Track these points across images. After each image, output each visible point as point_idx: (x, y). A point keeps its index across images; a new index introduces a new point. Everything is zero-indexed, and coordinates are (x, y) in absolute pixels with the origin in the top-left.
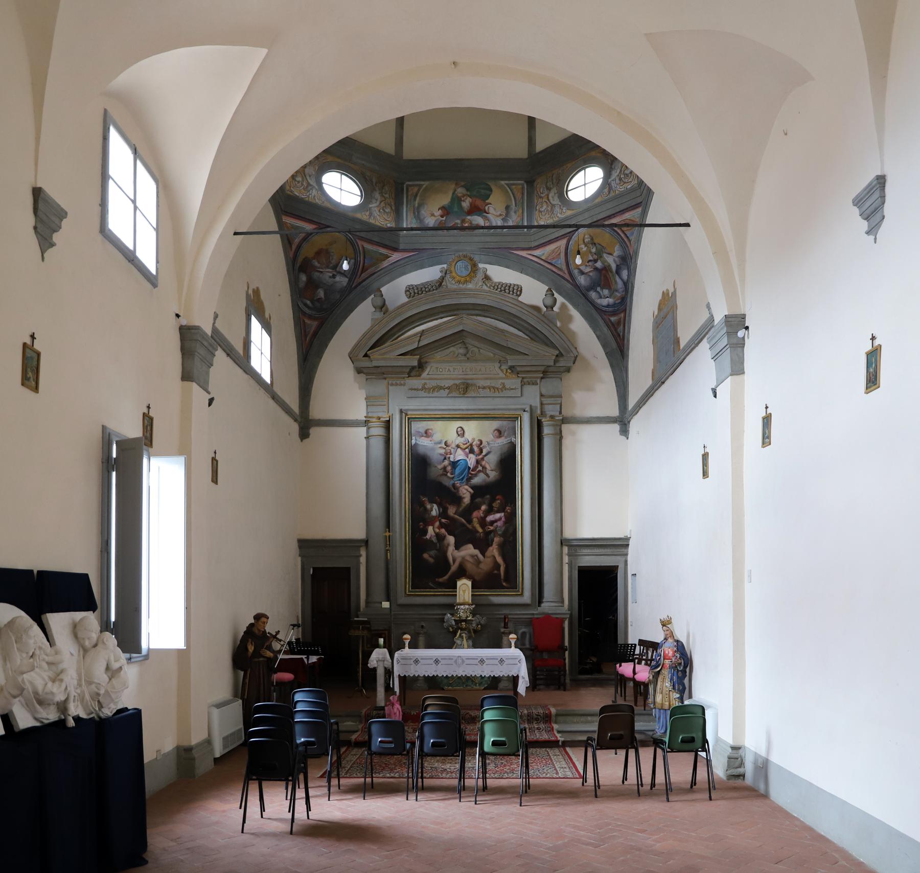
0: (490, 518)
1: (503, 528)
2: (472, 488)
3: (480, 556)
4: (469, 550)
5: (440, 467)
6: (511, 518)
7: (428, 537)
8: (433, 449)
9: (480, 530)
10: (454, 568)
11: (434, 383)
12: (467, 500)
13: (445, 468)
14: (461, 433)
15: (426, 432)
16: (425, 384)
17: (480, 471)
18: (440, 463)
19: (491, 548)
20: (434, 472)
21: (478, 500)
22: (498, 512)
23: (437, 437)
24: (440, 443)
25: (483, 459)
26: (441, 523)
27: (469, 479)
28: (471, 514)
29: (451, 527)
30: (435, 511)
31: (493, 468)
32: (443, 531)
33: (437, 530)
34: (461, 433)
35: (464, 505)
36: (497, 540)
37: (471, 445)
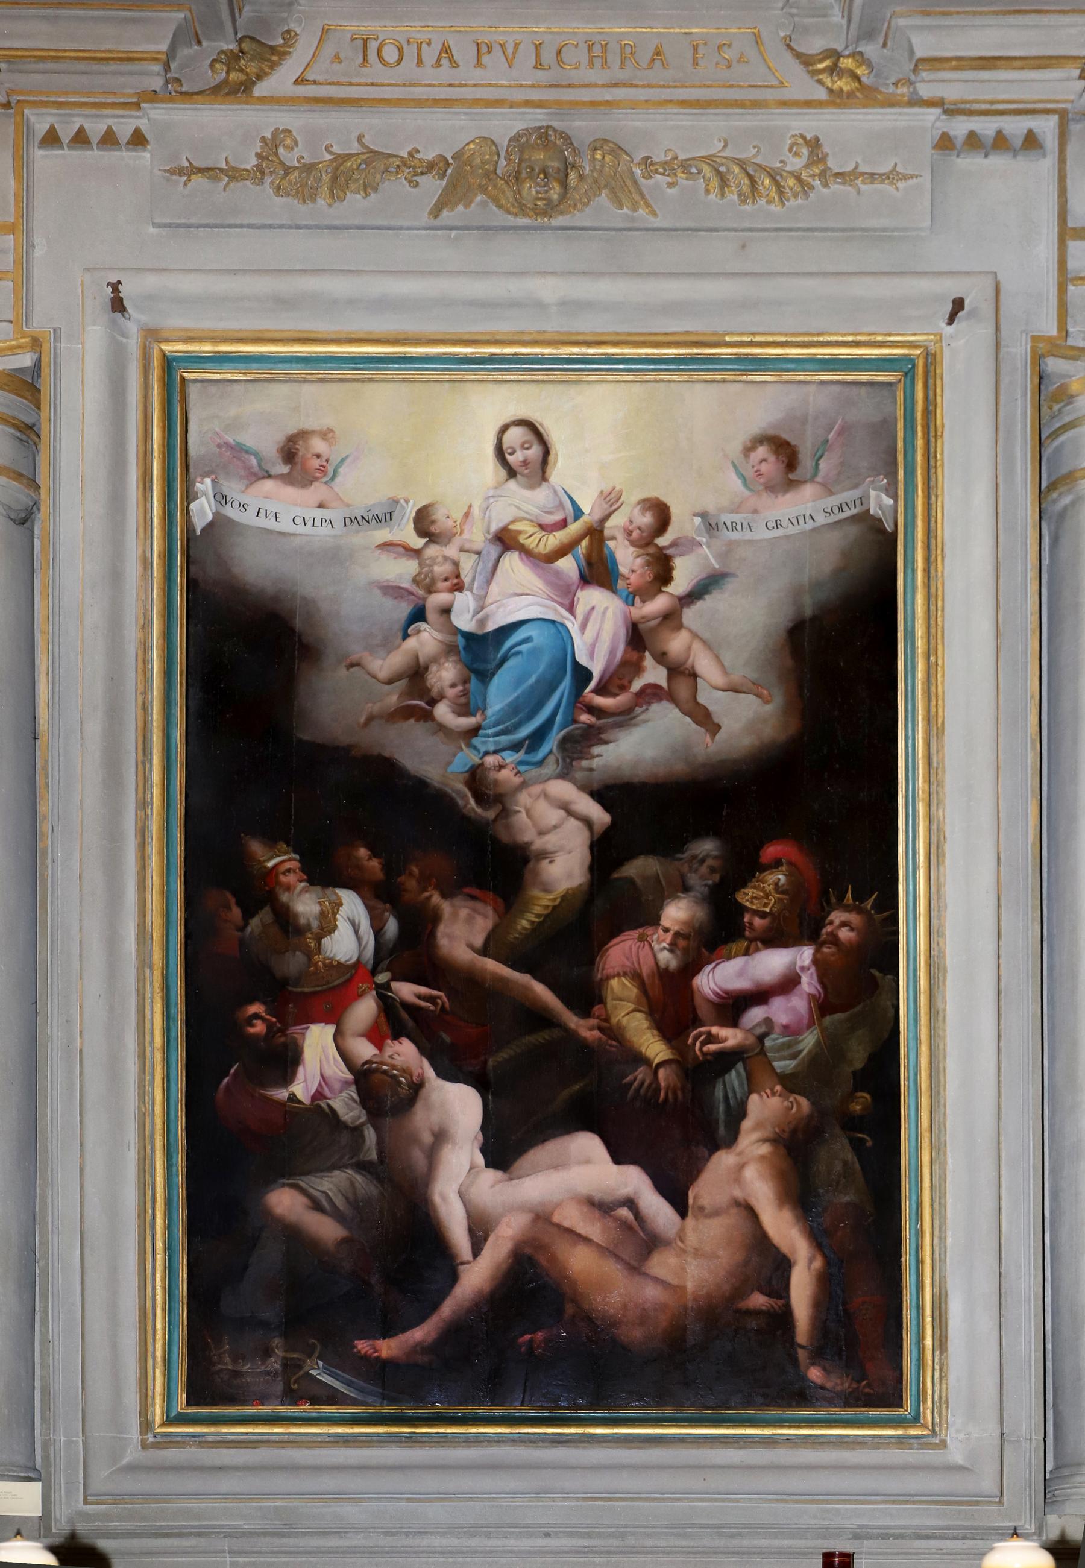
0: (720, 977)
1: (809, 1041)
2: (602, 794)
3: (657, 1208)
4: (579, 1170)
6: (864, 983)
7: (302, 1088)
8: (334, 557)
9: (656, 1049)
10: (476, 1275)
11: (342, 132)
12: (565, 867)
13: (416, 675)
14: (526, 454)
15: (290, 453)
16: (273, 143)
17: (652, 693)
18: (387, 646)
19: (723, 1160)
20: (344, 702)
21: (640, 868)
22: (774, 939)
23: (362, 483)
24: (385, 517)
25: (671, 618)
26: (388, 1005)
27: (578, 744)
29: (465, 1031)
30: (348, 930)
31: (741, 672)
32: (404, 1053)
33: (364, 1050)
34: (526, 454)
35: (541, 902)
36: (765, 1109)
37: (596, 533)
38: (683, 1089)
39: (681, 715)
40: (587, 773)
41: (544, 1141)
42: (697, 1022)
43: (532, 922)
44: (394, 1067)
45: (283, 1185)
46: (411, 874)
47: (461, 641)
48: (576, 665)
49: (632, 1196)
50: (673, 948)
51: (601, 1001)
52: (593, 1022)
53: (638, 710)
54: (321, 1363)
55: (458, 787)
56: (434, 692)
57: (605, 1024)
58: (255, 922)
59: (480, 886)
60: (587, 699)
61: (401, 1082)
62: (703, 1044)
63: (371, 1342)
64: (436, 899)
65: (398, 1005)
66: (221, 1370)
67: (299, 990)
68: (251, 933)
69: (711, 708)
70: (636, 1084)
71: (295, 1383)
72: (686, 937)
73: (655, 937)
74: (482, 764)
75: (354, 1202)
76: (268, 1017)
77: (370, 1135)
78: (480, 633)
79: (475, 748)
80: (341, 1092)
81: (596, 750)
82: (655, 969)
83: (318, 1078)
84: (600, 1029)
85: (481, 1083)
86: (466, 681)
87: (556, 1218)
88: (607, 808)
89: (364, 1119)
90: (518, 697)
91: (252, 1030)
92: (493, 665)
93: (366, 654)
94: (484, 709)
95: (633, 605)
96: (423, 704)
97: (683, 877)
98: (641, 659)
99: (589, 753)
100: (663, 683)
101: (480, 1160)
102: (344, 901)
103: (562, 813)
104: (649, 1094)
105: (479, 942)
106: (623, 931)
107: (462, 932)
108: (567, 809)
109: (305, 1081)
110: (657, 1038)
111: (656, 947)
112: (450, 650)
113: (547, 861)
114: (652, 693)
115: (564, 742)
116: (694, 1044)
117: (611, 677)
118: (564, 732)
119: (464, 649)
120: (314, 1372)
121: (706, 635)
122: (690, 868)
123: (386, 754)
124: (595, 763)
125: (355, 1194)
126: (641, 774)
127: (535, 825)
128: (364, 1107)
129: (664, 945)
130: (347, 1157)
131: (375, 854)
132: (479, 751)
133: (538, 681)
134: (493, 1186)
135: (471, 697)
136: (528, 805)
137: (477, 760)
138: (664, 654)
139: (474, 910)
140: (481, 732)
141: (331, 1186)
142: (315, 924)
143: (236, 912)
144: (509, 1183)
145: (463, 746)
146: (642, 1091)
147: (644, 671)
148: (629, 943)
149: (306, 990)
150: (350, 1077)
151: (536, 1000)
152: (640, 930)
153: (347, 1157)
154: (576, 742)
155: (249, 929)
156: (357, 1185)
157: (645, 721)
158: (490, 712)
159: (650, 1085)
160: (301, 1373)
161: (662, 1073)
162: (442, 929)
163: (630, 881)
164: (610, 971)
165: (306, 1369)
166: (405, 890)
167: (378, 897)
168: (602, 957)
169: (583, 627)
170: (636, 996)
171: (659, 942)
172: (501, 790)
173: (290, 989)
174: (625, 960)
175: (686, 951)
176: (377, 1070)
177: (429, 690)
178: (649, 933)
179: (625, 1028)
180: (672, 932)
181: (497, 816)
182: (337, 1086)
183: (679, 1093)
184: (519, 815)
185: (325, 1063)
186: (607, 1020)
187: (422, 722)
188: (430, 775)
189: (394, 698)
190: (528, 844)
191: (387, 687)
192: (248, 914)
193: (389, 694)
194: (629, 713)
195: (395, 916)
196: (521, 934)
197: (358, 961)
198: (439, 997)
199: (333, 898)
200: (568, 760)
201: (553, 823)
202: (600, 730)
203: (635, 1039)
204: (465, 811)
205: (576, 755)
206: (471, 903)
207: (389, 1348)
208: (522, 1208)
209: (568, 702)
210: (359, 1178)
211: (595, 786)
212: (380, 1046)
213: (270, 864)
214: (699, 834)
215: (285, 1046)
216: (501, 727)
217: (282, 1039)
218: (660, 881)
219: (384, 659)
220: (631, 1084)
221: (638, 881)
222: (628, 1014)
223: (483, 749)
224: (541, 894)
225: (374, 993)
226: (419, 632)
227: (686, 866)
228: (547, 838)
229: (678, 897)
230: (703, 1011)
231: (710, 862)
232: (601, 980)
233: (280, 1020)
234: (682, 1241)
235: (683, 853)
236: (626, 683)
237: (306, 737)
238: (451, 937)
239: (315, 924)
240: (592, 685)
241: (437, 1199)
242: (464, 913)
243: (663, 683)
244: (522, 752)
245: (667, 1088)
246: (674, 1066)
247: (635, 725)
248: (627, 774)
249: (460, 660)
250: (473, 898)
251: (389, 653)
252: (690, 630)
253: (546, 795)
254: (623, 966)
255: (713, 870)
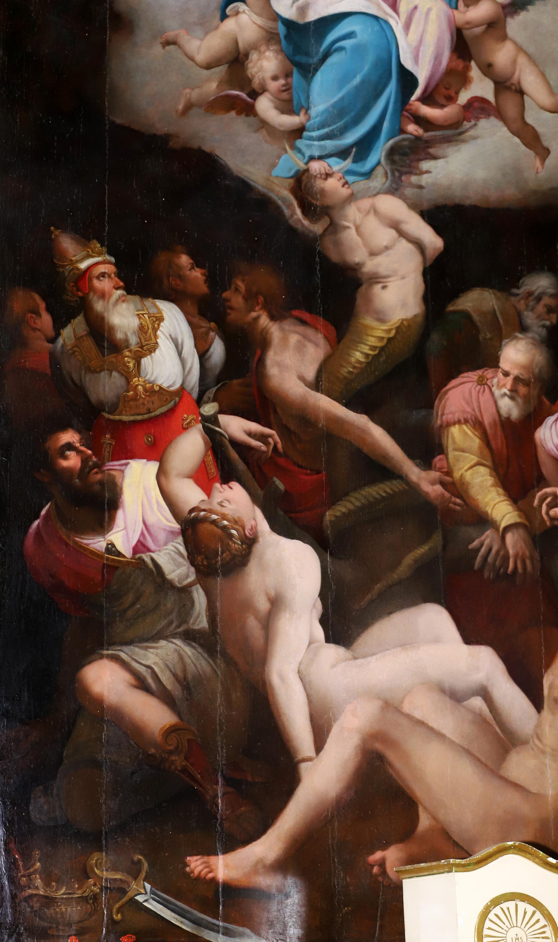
5: (205, 45)
7: (122, 536)
9: (501, 510)
10: (323, 777)
13: (235, 61)
17: (478, 108)
18: (205, 26)
21: (476, 301)
26: (216, 441)
27: (407, 157)
28: (427, 396)
29: (301, 478)
30: (170, 351)
32: (235, 501)
33: (191, 495)
38: (532, 558)
39: (510, 134)
40: (416, 190)
41: (390, 613)
42: (542, 481)
43: (367, 355)
44: (224, 517)
45: (102, 657)
46: (237, 290)
47: (282, 30)
48: (402, 69)
49: (485, 682)
50: (513, 394)
51: (441, 450)
52: (434, 475)
53: (467, 125)
54: (148, 886)
55: (283, 194)
56: (256, 83)
57: (448, 479)
58: (67, 332)
59: (310, 311)
60: (413, 108)
61: (231, 536)
62: (551, 506)
63: (206, 859)
64: (264, 320)
65: (227, 443)
66: (31, 896)
67: (117, 417)
68: (63, 346)
69: (540, 130)
70: (483, 550)
71: (118, 911)
72: (527, 383)
73: (495, 381)
74: (307, 170)
75: (184, 682)
76: (83, 448)
77: (199, 597)
78: (301, 22)
79: (300, 151)
80: (166, 544)
81: (425, 165)
82: (497, 418)
83: (141, 525)
84: (443, 484)
85: (320, 542)
86: (288, 75)
87: (407, 708)
88: (438, 230)
89: (192, 577)
90: (342, 98)
91: (65, 463)
92: (315, 60)
93: (182, 32)
94: (307, 109)
95: (456, 8)
96: (244, 95)
97: (519, 314)
98: (467, 68)
99: (418, 168)
100: (491, 97)
101: (320, 633)
102: (165, 316)
103: (393, 233)
104: (498, 563)
105: (311, 374)
106: (463, 373)
107: (293, 361)
108: (396, 226)
109: (125, 528)
110: (503, 498)
111: (497, 393)
112: (271, 37)
113: (380, 286)
114: (478, 108)
115: (392, 153)
116: (540, 506)
117: (437, 86)
118: (391, 142)
119: (286, 37)
120: (140, 898)
121: (531, 50)
122: (527, 305)
123: (206, 148)
124: (425, 179)
125: (185, 671)
126: (472, 197)
127: (366, 244)
128: (192, 563)
129: (505, 390)
130: (174, 625)
131: (198, 263)
132: (303, 155)
133: (363, 82)
134: (333, 666)
135: (294, 93)
136: (358, 222)
137: (302, 165)
138: (490, 65)
139: (305, 337)
140: (305, 134)
141: (157, 660)
142: (133, 340)
143: (46, 320)
144: (353, 663)
145: (287, 148)
146: (490, 559)
147: (470, 82)
148: (469, 385)
149: (125, 418)
150: (176, 526)
151: (375, 446)
152: (480, 372)
153: (174, 625)
154: (405, 154)
155: (60, 341)
156: (188, 661)
157: (475, 138)
158: (313, 112)
159: (498, 552)
160: (125, 899)
161: (510, 538)
162: (271, 357)
163: (466, 315)
164: (448, 417)
165: (130, 894)
166: (231, 308)
167: (202, 314)
168: (440, 401)
169: (407, 26)
170: (480, 448)
171: (500, 387)
172: (328, 201)
173: (106, 415)
174: (465, 405)
175: (527, 399)
176: (204, 520)
177: (249, 81)
178: (489, 376)
179: (468, 484)
180: (512, 377)
181: (325, 231)
182: (162, 536)
183: (528, 562)
184: (348, 231)
185: (147, 507)
186: (449, 473)
187: (243, 116)
188: (253, 177)
189: (213, 86)
190: (359, 266)
191: (205, 72)
192: (60, 323)
193: (208, 80)
194: (457, 128)
195: (221, 338)
196: (354, 367)
197: (182, 388)
198: (270, 436)
199: (153, 311)
200: (397, 174)
201: (385, 243)
202: (429, 143)
203: (479, 497)
204: (291, 222)
205: (404, 169)
206: (301, 329)
207: (226, 866)
208: (369, 693)
209: (395, 110)
210: (188, 650)
211: (425, 206)
212: (208, 491)
213: (83, 266)
214: (534, 268)
215: (101, 483)
216: (326, 130)
217: (99, 476)
218: (497, 318)
219: (202, 40)
220: (478, 550)
221: (476, 317)
222: (471, 467)
223: (308, 153)
224: (375, 324)
225: (200, 426)
226: (237, 13)
227: (523, 302)
228: (379, 260)
229: (516, 338)
230: (547, 468)
231: (546, 300)
232: (441, 426)
233: (94, 454)
234: (540, 740)
235: (518, 288)
236: (452, 93)
237: (118, 121)
238: (279, 365)
239: (133, 340)
240: (418, 92)
241: (275, 679)
242: (294, 339)
243: (491, 97)
244: (349, 160)
245: (516, 556)
246: (521, 531)
247: (464, 141)
248: (459, 195)
249: (282, 50)
250: (303, 322)
251: (207, 33)
252: (515, 43)
253: (376, 212)
254: (464, 412)
255: (550, 310)
